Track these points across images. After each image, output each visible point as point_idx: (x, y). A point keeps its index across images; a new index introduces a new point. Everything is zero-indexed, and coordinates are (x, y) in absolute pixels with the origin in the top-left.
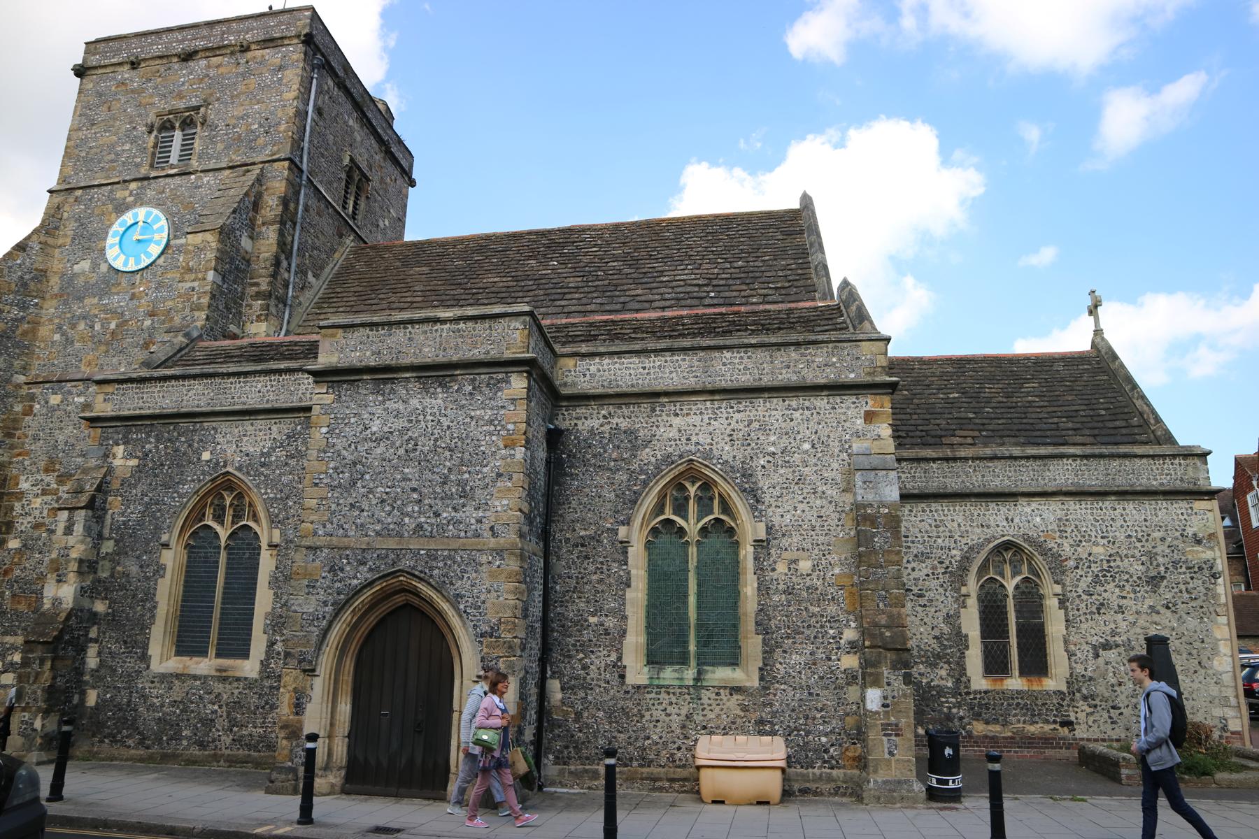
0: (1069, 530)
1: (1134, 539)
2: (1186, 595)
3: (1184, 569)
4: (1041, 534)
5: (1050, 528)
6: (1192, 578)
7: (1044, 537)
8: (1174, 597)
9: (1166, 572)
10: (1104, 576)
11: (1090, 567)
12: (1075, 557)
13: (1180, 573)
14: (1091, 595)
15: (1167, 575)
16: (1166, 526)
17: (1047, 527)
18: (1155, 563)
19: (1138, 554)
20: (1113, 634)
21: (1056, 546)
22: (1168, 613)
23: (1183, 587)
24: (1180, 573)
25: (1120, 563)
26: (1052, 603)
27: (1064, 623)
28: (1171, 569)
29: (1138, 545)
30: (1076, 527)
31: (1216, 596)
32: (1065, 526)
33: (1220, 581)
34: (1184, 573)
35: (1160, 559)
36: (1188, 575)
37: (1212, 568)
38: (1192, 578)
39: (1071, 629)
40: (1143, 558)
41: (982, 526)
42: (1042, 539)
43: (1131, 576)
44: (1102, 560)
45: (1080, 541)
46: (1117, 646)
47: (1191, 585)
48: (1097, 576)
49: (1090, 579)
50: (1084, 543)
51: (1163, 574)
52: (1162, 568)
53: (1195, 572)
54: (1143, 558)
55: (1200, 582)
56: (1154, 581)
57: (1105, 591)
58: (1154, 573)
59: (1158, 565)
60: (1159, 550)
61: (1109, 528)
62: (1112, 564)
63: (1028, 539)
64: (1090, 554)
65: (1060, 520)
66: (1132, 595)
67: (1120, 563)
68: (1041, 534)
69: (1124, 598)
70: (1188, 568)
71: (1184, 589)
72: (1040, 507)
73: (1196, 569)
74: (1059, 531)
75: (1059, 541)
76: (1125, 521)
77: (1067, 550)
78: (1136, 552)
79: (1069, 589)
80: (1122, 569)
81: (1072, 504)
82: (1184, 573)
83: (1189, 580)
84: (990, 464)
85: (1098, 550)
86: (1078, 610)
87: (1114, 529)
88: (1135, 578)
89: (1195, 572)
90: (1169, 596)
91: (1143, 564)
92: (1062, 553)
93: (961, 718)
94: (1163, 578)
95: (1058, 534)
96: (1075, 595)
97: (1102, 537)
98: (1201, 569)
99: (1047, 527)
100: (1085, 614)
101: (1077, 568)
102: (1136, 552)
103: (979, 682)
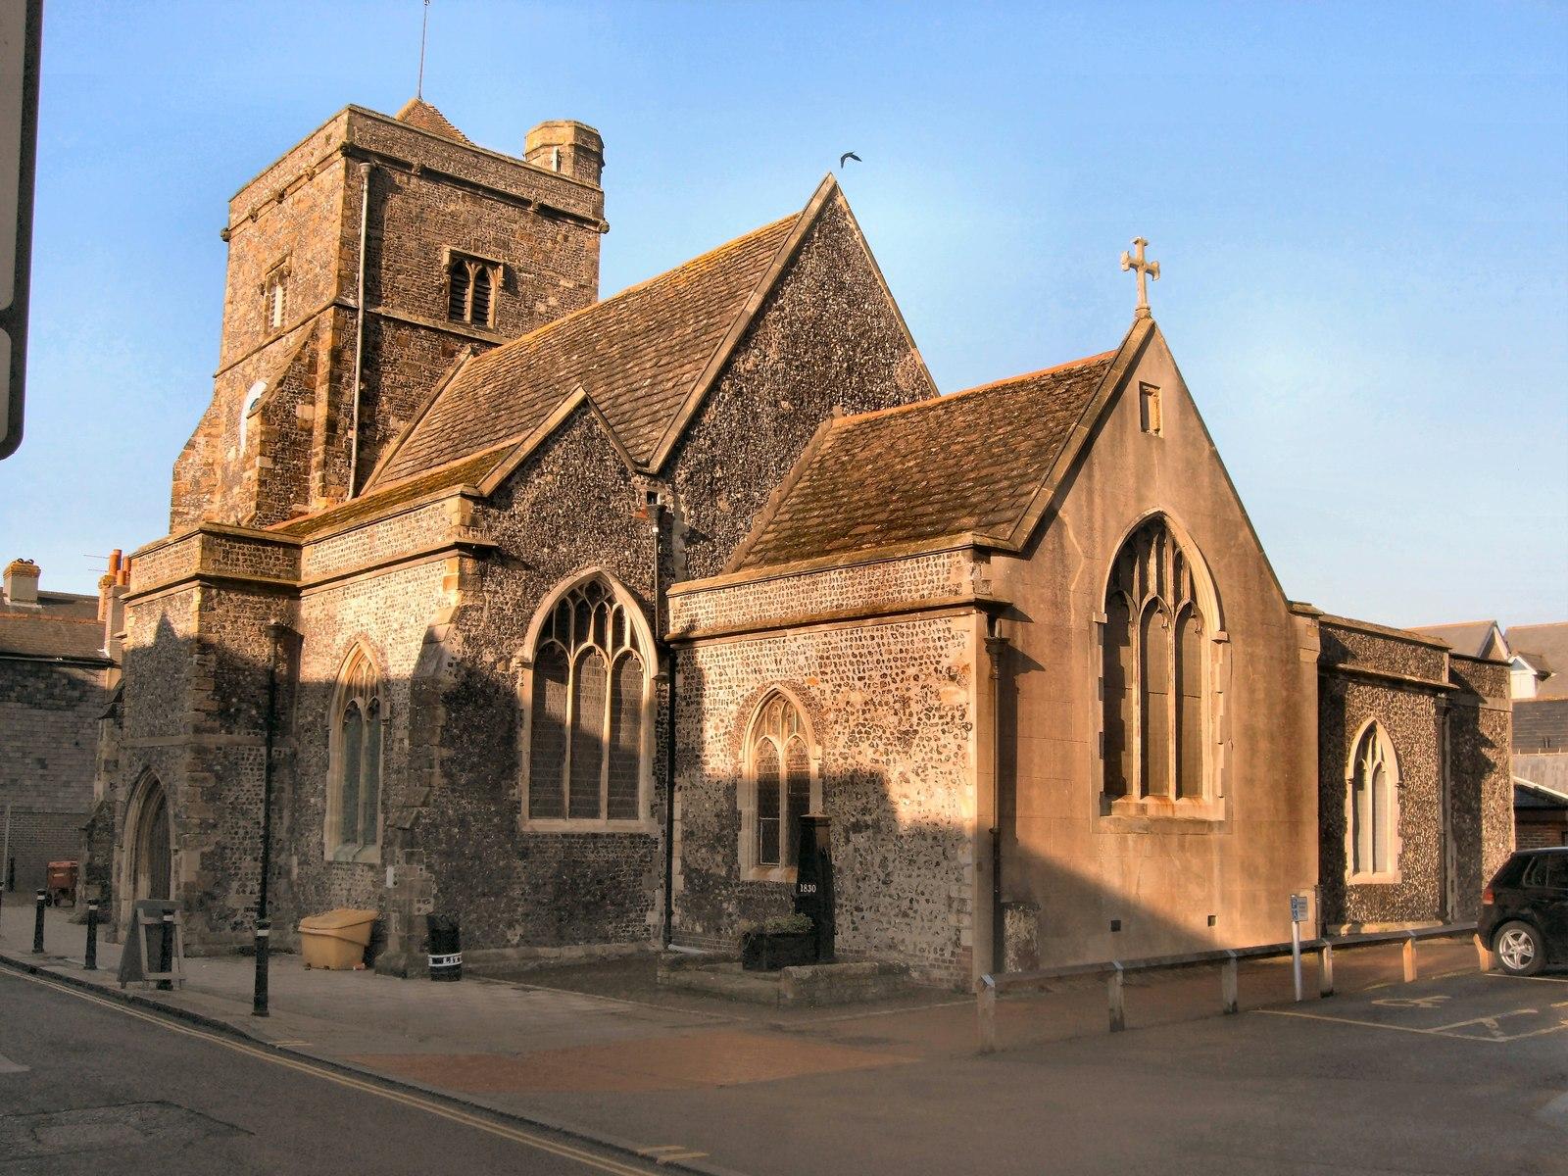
6: (944, 732)
9: (919, 724)
12: (835, 707)
13: (932, 725)
16: (921, 658)
18: (907, 711)
19: (892, 701)
21: (818, 693)
24: (932, 725)
25: (875, 714)
28: (924, 720)
34: (937, 724)
37: (963, 716)
43: (884, 732)
45: (840, 685)
46: (867, 827)
51: (915, 728)
52: (915, 720)
54: (897, 706)
55: (952, 735)
59: (911, 715)
60: (911, 694)
64: (848, 703)
69: (877, 761)
84: (767, 588)
93: (730, 915)
101: (836, 722)
103: (749, 873)
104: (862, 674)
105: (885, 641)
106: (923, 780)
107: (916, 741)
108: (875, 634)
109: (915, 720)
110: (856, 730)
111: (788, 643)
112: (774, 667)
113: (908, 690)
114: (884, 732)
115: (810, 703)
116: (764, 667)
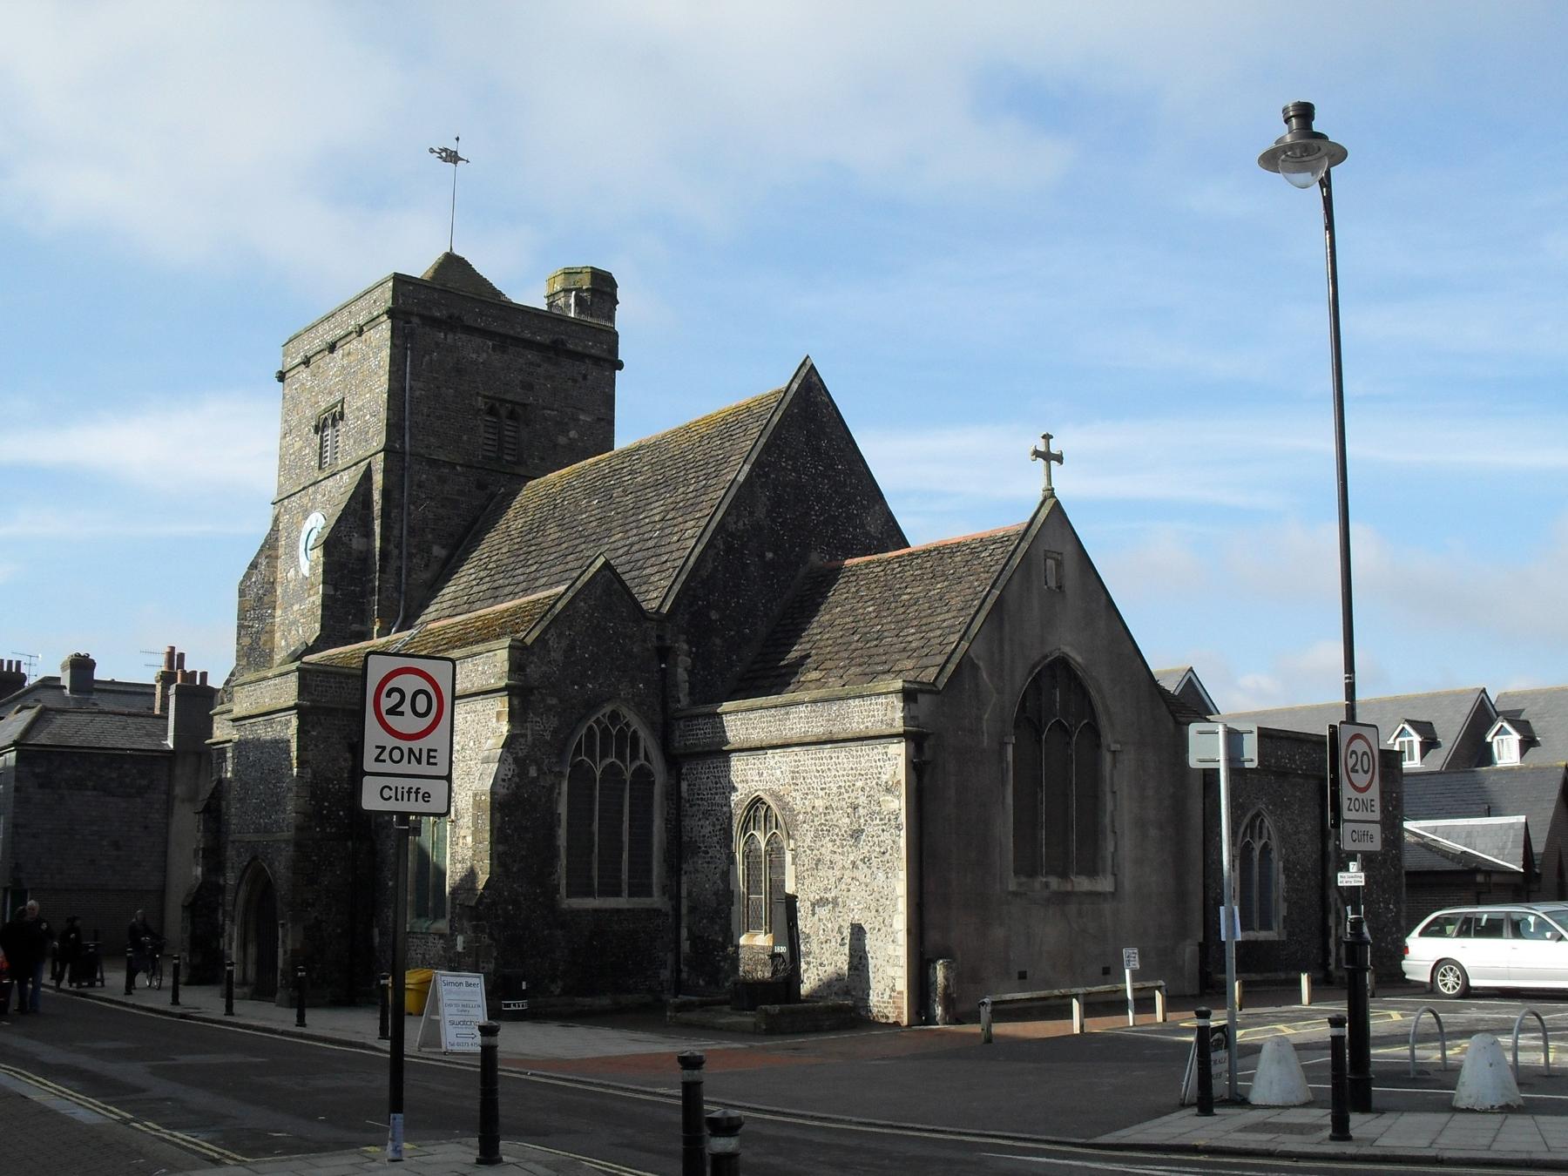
0: (799, 782)
1: (843, 790)
2: (877, 849)
3: (878, 821)
5: (787, 781)
6: (883, 831)
11: (813, 821)
12: (804, 810)
20: (826, 890)
23: (875, 839)
24: (874, 825)
29: (846, 796)
31: (898, 849)
33: (902, 832)
34: (878, 825)
35: (861, 811)
37: (897, 818)
38: (883, 831)
39: (799, 885)
43: (840, 830)
44: (821, 814)
45: (807, 794)
47: (882, 838)
50: (809, 797)
51: (862, 827)
52: (862, 821)
53: (885, 824)
56: (856, 834)
57: (822, 846)
58: (855, 826)
59: (859, 817)
61: (826, 779)
62: (828, 817)
64: (814, 807)
67: (833, 817)
68: (781, 787)
70: (881, 820)
73: (886, 821)
74: (793, 784)
75: (794, 794)
78: (844, 803)
79: (799, 844)
80: (835, 823)
85: (819, 803)
87: (830, 779)
89: (885, 824)
91: (848, 817)
97: (822, 789)
98: (889, 820)
100: (807, 870)
102: (844, 803)
104: (824, 786)
105: (840, 760)
106: (868, 867)
107: (863, 837)
108: (833, 755)
109: (862, 821)
110: (820, 829)
111: (768, 759)
112: (757, 778)
113: (856, 798)
114: (840, 830)
115: (784, 807)
116: (749, 778)
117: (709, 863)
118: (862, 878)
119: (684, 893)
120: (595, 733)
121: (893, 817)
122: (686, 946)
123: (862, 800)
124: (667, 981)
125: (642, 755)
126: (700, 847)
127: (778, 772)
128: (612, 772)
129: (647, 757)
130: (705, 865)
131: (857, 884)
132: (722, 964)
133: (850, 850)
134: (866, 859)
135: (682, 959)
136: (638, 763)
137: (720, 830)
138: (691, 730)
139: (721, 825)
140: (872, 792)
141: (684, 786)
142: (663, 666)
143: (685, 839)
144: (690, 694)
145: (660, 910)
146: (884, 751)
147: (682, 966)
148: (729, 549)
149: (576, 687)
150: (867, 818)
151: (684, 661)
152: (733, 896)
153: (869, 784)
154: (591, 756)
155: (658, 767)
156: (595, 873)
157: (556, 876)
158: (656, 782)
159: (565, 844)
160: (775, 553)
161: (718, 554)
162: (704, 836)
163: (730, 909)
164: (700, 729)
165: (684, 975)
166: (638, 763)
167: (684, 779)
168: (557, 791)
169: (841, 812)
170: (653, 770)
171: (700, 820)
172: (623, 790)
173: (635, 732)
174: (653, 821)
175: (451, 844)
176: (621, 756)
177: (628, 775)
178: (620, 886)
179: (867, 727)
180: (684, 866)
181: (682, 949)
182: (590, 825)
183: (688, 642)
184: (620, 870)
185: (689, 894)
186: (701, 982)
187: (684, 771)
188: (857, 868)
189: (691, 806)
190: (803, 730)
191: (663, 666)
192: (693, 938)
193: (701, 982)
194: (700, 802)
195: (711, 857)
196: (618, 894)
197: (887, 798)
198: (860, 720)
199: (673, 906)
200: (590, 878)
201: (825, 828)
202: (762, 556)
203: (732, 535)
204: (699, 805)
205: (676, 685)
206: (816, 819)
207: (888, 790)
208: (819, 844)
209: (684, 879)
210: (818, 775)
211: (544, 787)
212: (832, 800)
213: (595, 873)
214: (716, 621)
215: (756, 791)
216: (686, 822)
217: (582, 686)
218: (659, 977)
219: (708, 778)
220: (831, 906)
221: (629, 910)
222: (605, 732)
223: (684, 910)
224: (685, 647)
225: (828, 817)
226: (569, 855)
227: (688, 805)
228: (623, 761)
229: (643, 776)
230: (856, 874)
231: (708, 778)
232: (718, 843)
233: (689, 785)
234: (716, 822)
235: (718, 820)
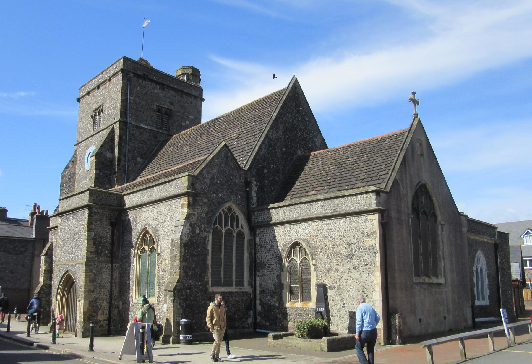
2: (363, 263)
4: (308, 237)
5: (311, 234)
7: (310, 238)
8: (358, 264)
10: (331, 255)
11: (326, 251)
13: (361, 252)
14: (326, 264)
15: (355, 253)
17: (310, 234)
22: (356, 271)
24: (361, 252)
26: (312, 268)
27: (316, 277)
28: (358, 250)
30: (321, 233)
32: (317, 233)
34: (363, 252)
35: (353, 246)
36: (364, 253)
38: (366, 254)
40: (346, 246)
41: (288, 236)
42: (309, 240)
47: (365, 258)
48: (328, 255)
49: (325, 257)
50: (324, 241)
51: (354, 253)
52: (354, 250)
56: (350, 256)
58: (350, 253)
59: (352, 249)
63: (304, 240)
64: (326, 245)
65: (315, 230)
66: (341, 264)
68: (308, 237)
71: (362, 260)
72: (308, 225)
74: (315, 235)
76: (339, 229)
77: (318, 245)
81: (320, 223)
82: (363, 252)
83: (364, 255)
86: (321, 271)
88: (343, 256)
90: (356, 263)
92: (316, 245)
94: (354, 255)
95: (314, 237)
96: (320, 264)
98: (369, 249)
99: (310, 234)
101: (321, 252)
117: (270, 271)
118: (354, 276)
119: (258, 284)
120: (222, 216)
121: (371, 248)
122: (259, 308)
123: (353, 241)
124: (251, 323)
125: (240, 226)
126: (266, 265)
127: (307, 231)
128: (229, 233)
129: (242, 227)
130: (269, 273)
131: (351, 279)
132: (278, 315)
133: (347, 264)
134: (356, 268)
135: (257, 313)
136: (238, 229)
137: (276, 257)
138: (260, 216)
139: (277, 255)
140: (359, 237)
141: (257, 239)
142: (248, 189)
143: (258, 261)
144: (257, 202)
145: (247, 292)
146: (365, 218)
147: (257, 316)
148: (270, 145)
149: (215, 195)
150: (356, 249)
151: (255, 189)
152: (283, 286)
153: (357, 234)
154: (220, 224)
155: (246, 231)
156: (222, 276)
157: (207, 277)
158: (246, 237)
159: (211, 263)
160: (286, 149)
161: (266, 146)
162: (268, 260)
163: (282, 291)
164: (265, 215)
165: (258, 321)
166: (238, 229)
167: (257, 237)
168: (207, 239)
169: (341, 247)
170: (244, 233)
171: (265, 253)
172: (233, 240)
173: (237, 216)
174: (244, 254)
175: (158, 263)
176: (232, 226)
177: (235, 234)
178: (232, 281)
179: (356, 208)
180: (258, 273)
181: (257, 309)
182: (220, 255)
183: (256, 181)
184: (231, 275)
185: (261, 285)
186: (267, 324)
187: (257, 233)
188: (351, 272)
189: (261, 247)
190: (320, 211)
191: (248, 189)
192: (262, 304)
193: (267, 324)
194: (266, 246)
195: (272, 269)
196: (231, 285)
197: (367, 239)
198: (351, 206)
199: (252, 290)
200: (221, 278)
201: (332, 254)
202: (281, 150)
203: (271, 139)
204: (265, 247)
205: (252, 198)
206: (327, 251)
207: (368, 236)
208: (329, 261)
209: (258, 279)
210: (328, 231)
211: (202, 237)
212: (337, 241)
213: (222, 276)
214: (266, 173)
215: (295, 239)
216: (258, 254)
217: (217, 195)
218: (247, 321)
219: (270, 235)
220: (336, 289)
221: (236, 292)
222: (226, 215)
223: (258, 292)
224: (255, 183)
225: (334, 249)
226: (212, 268)
227: (259, 247)
228: (233, 228)
229: (241, 235)
230: (350, 274)
231: (270, 235)
232: (275, 263)
233: (260, 239)
234: (274, 254)
235: (275, 253)
